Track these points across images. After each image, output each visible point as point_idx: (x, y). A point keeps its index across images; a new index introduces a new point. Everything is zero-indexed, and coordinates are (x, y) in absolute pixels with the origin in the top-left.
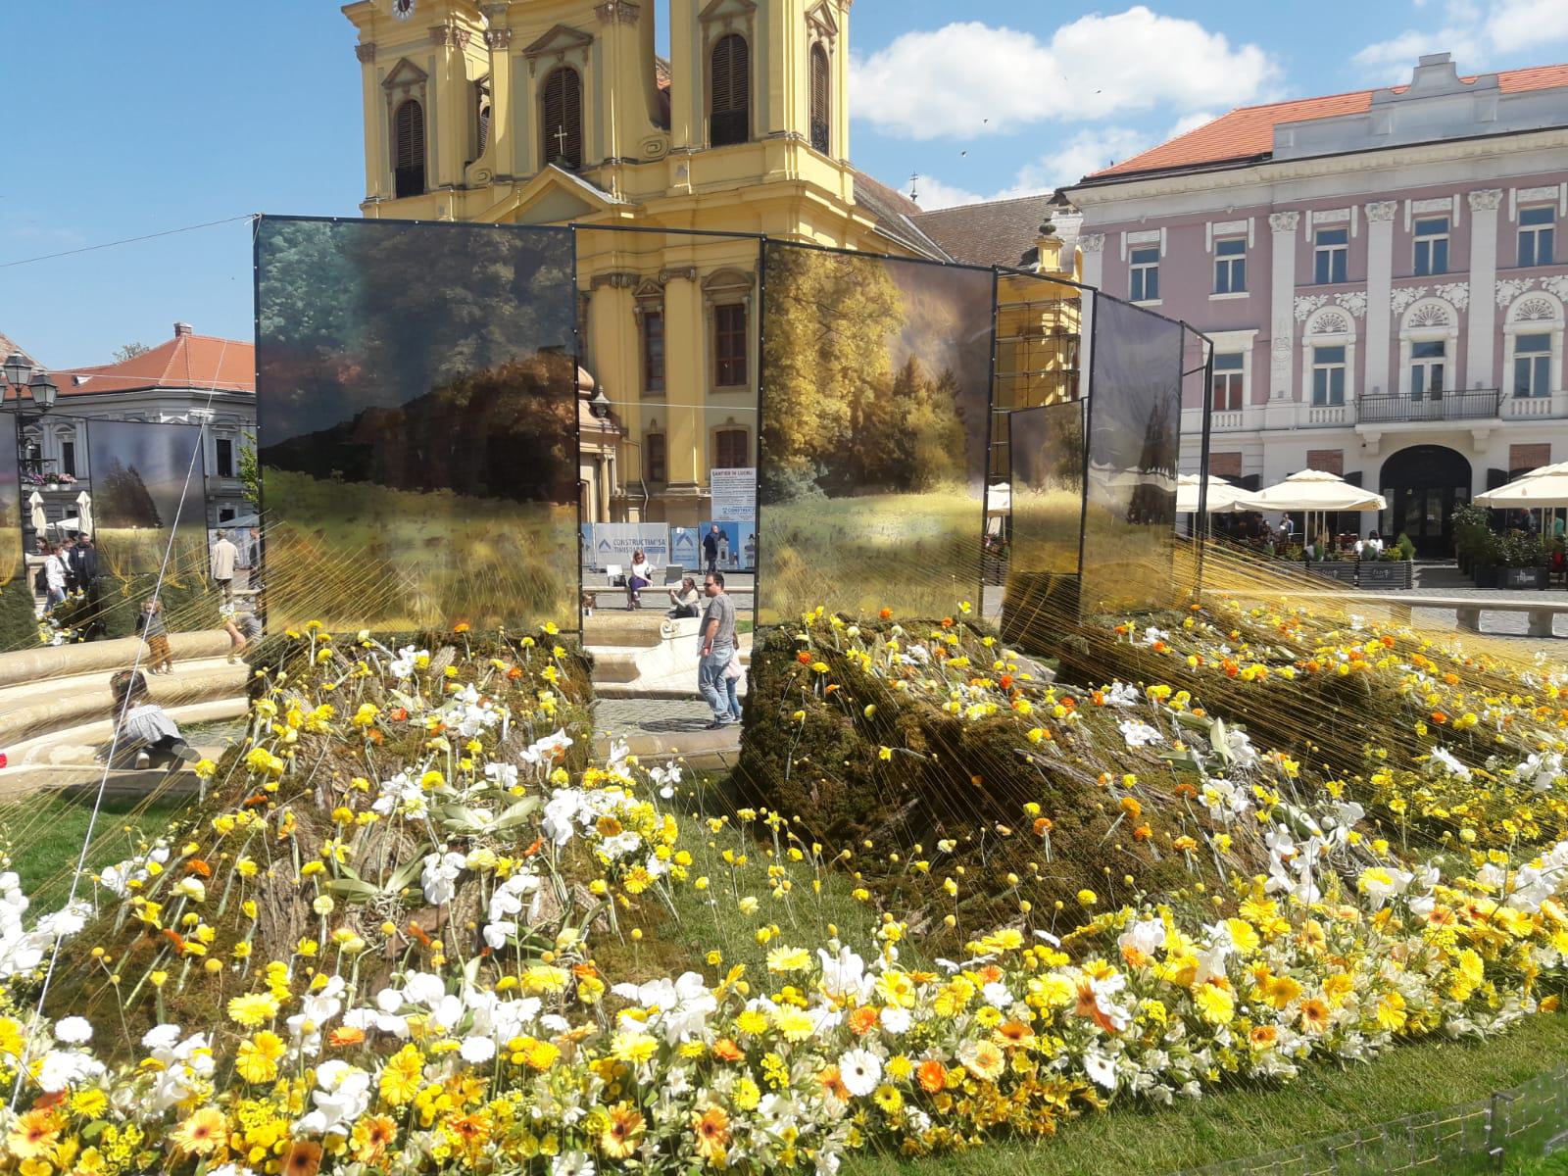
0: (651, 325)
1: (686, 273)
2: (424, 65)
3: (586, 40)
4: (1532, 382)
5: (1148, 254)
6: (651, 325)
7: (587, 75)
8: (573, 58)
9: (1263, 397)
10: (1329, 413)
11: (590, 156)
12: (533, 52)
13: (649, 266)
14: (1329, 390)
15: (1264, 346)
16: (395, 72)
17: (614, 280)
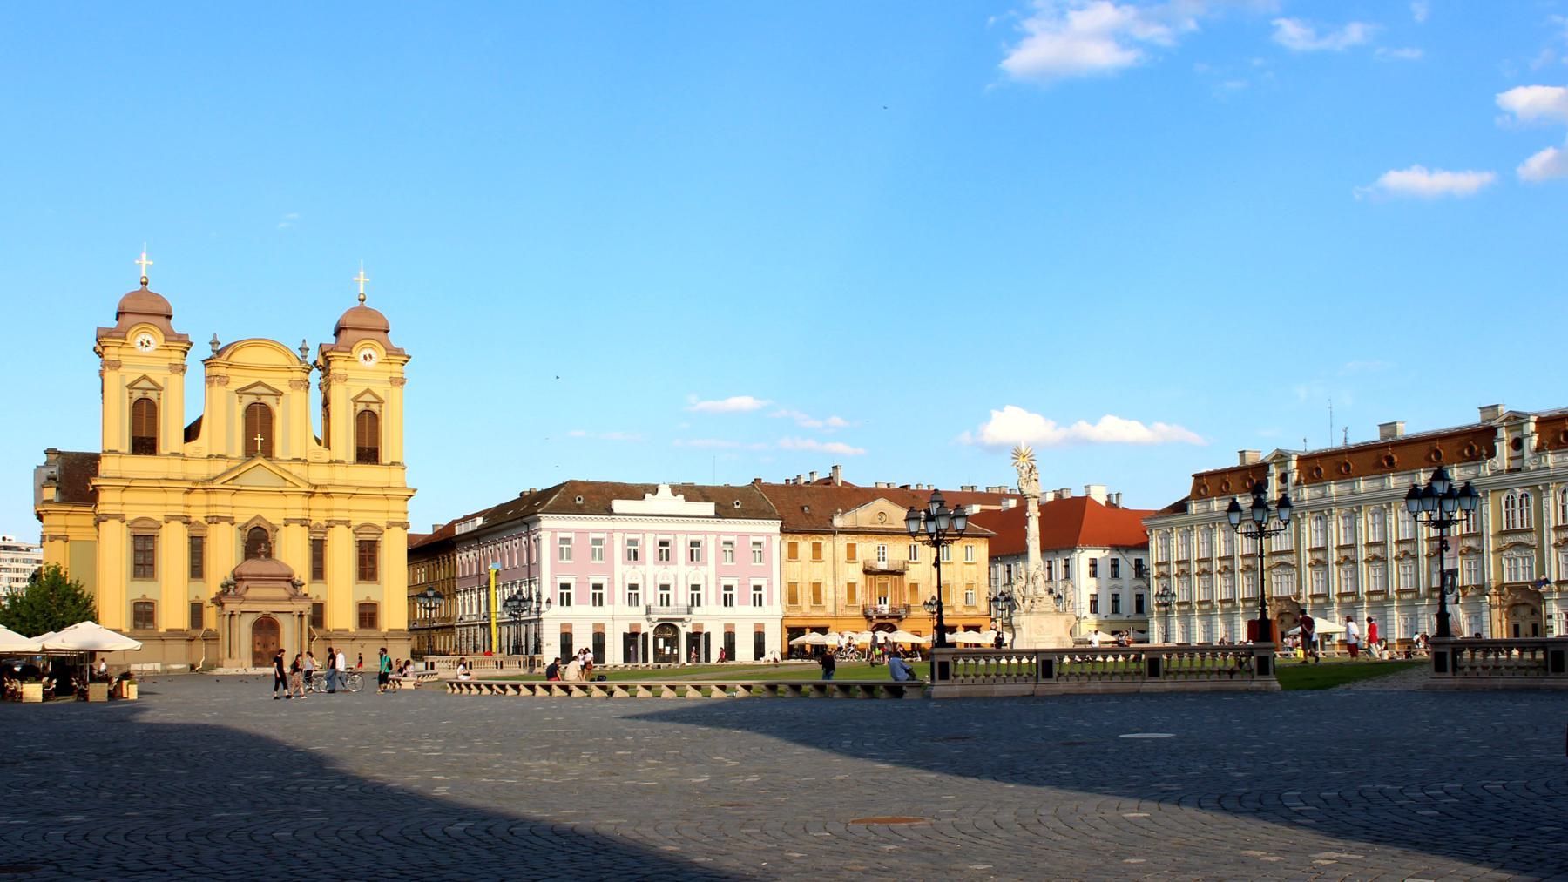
0: (318, 549)
1: (347, 524)
2: (161, 383)
3: (278, 394)
4: (696, 601)
5: (567, 540)
6: (318, 549)
7: (278, 412)
8: (270, 401)
9: (612, 602)
10: (634, 610)
11: (278, 451)
12: (241, 392)
13: (319, 518)
14: (633, 600)
15: (611, 583)
16: (138, 381)
17: (304, 523)
